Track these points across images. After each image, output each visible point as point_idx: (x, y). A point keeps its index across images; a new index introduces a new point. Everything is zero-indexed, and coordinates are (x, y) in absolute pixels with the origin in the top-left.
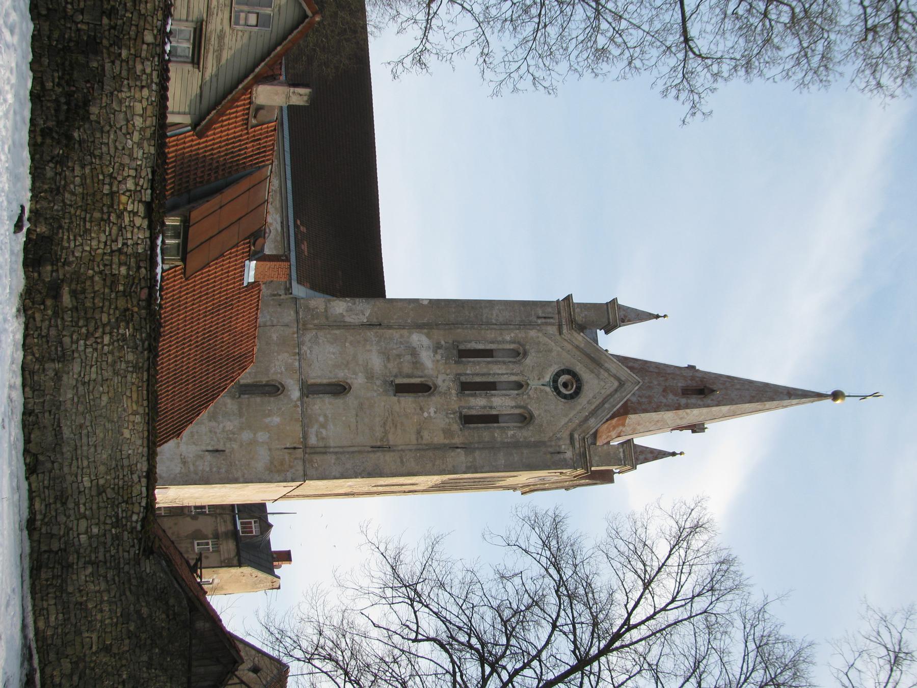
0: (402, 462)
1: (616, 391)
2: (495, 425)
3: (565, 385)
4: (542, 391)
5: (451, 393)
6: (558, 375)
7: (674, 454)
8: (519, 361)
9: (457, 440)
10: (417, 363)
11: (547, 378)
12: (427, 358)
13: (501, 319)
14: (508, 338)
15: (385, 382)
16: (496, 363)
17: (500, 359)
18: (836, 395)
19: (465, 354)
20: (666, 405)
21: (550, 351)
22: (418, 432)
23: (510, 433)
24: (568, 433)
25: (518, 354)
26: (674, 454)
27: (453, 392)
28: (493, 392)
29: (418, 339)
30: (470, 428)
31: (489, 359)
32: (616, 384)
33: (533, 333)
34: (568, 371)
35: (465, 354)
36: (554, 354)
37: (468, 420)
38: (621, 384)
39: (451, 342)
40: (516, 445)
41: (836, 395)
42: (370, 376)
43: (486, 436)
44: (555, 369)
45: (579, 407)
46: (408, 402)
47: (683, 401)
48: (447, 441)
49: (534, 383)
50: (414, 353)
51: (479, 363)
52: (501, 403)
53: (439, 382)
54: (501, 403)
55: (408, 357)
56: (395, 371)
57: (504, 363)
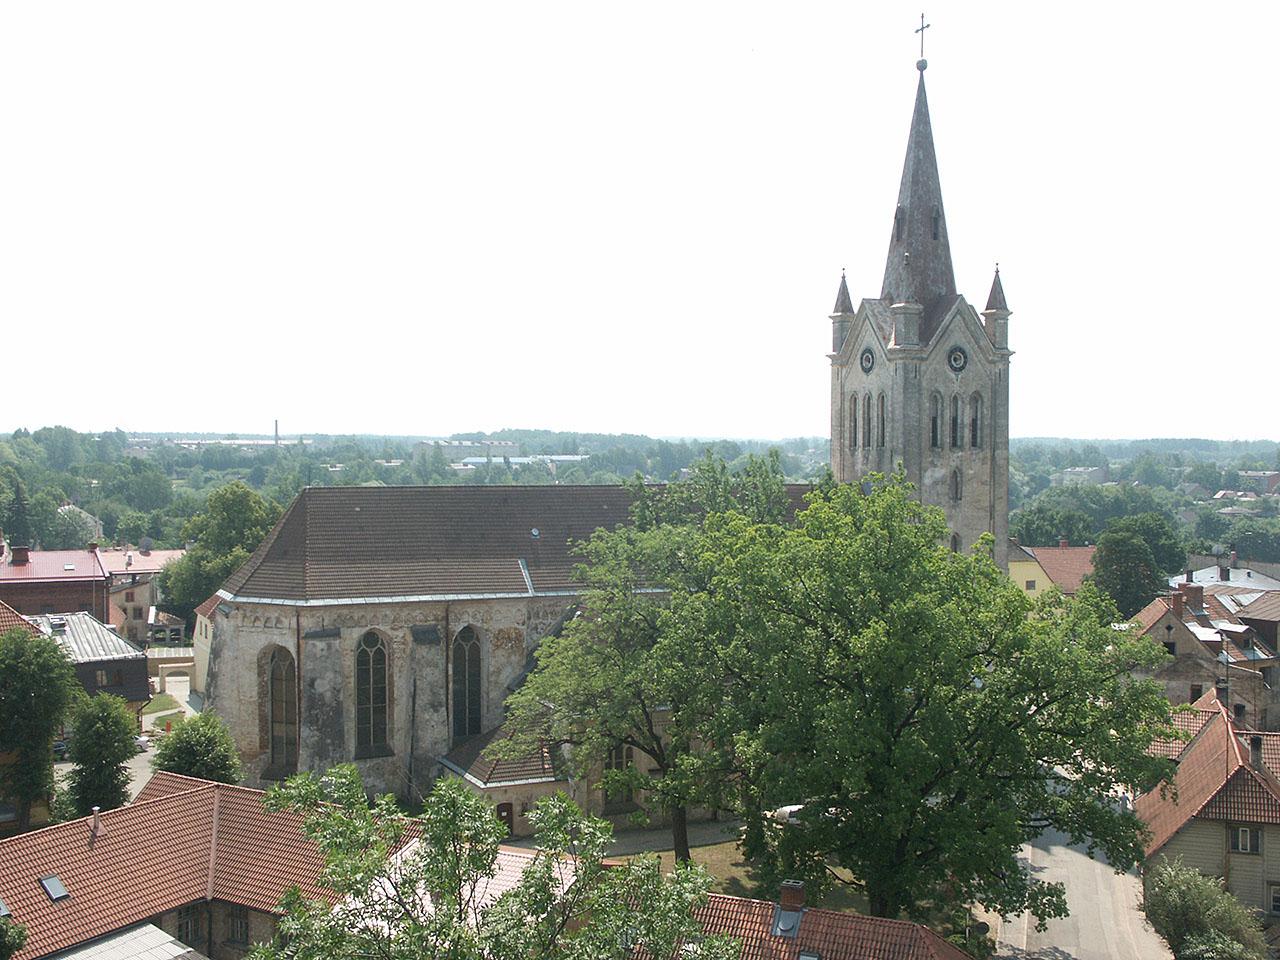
0: (1001, 498)
1: (964, 319)
2: (979, 422)
3: (955, 360)
4: (961, 382)
5: (962, 456)
6: (952, 366)
7: (997, 272)
8: (942, 398)
9: (989, 455)
10: (942, 481)
11: (953, 375)
12: (940, 472)
13: (918, 410)
14: (928, 404)
15: (954, 507)
16: (942, 418)
17: (939, 412)
18: (922, 66)
19: (934, 444)
20: (946, 259)
21: (935, 370)
22: (983, 484)
23: (985, 412)
24: (987, 364)
25: (935, 397)
26: (997, 272)
27: (960, 454)
28: (959, 421)
29: (927, 481)
30: (981, 447)
31: (939, 422)
32: (958, 317)
33: (924, 384)
34: (950, 357)
35: (934, 444)
36: (938, 366)
37: (974, 444)
38: (959, 312)
39: (929, 453)
40: (994, 407)
41: (922, 66)
42: (950, 517)
43: (987, 431)
44: (947, 368)
45: (972, 352)
46: (967, 490)
47: (942, 239)
48: (989, 463)
49: (956, 388)
50: (936, 483)
51: (942, 431)
52: (966, 418)
53: (953, 464)
54: (966, 418)
55: (939, 487)
56: (946, 497)
57: (943, 411)
